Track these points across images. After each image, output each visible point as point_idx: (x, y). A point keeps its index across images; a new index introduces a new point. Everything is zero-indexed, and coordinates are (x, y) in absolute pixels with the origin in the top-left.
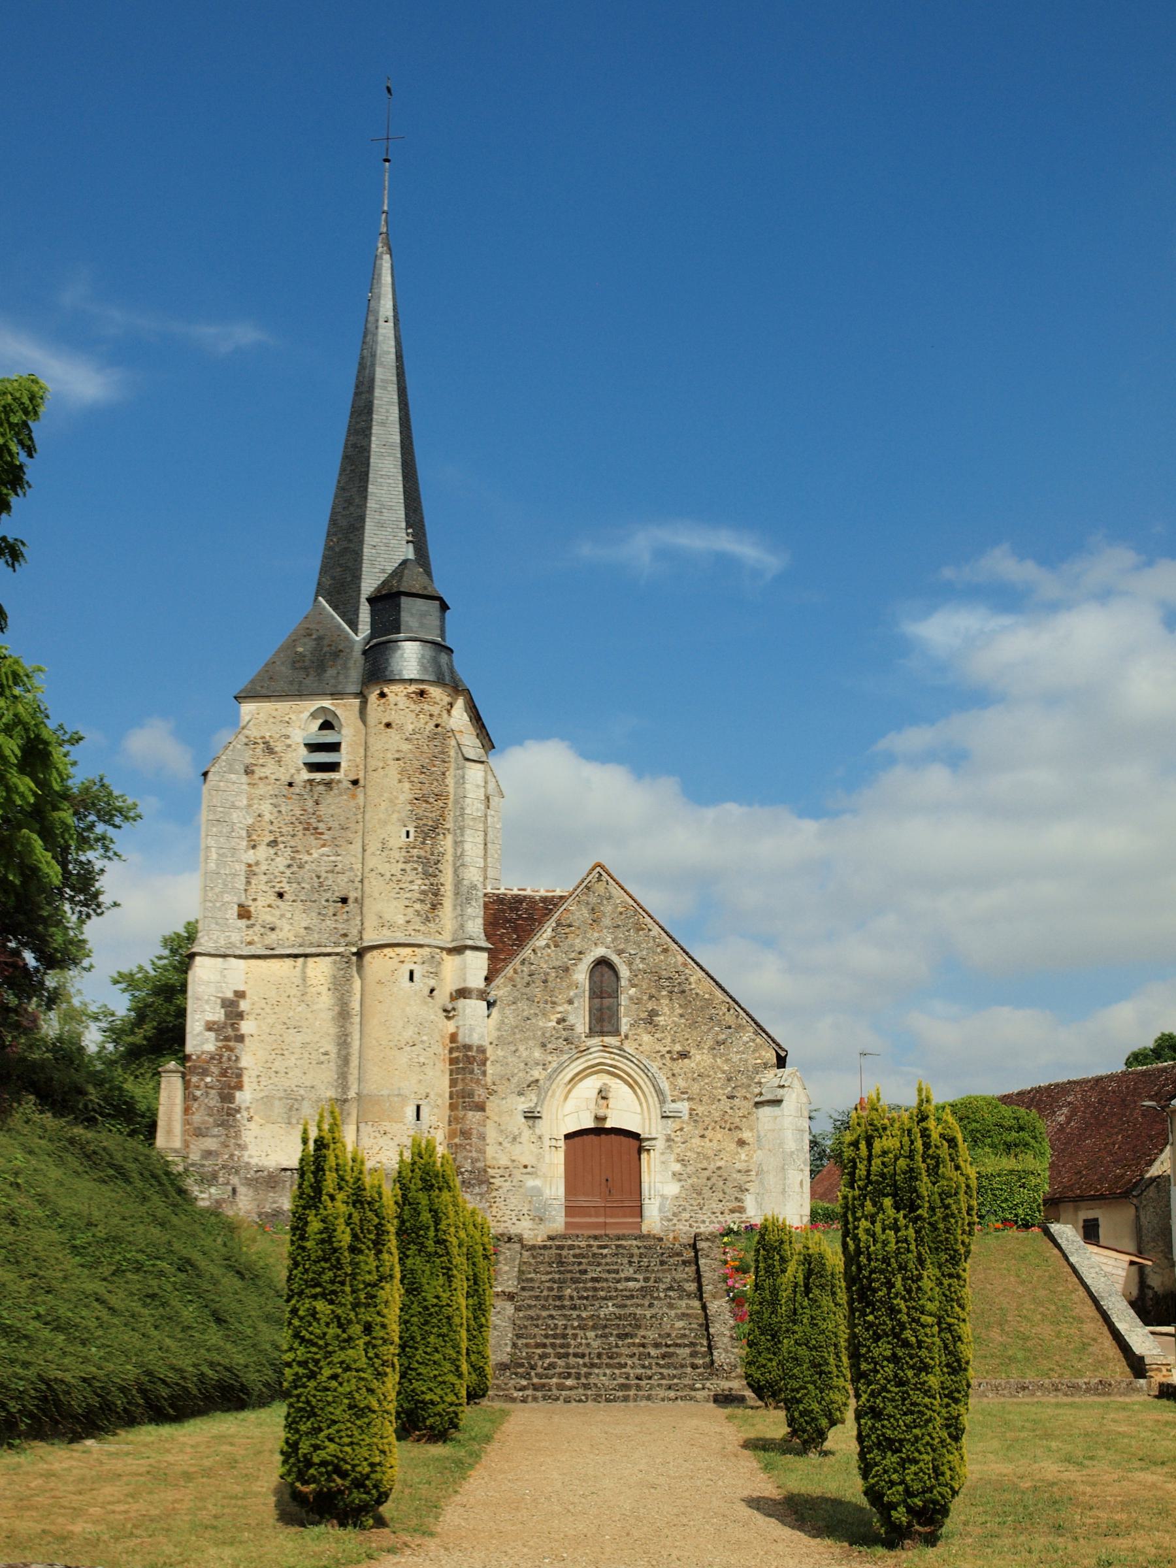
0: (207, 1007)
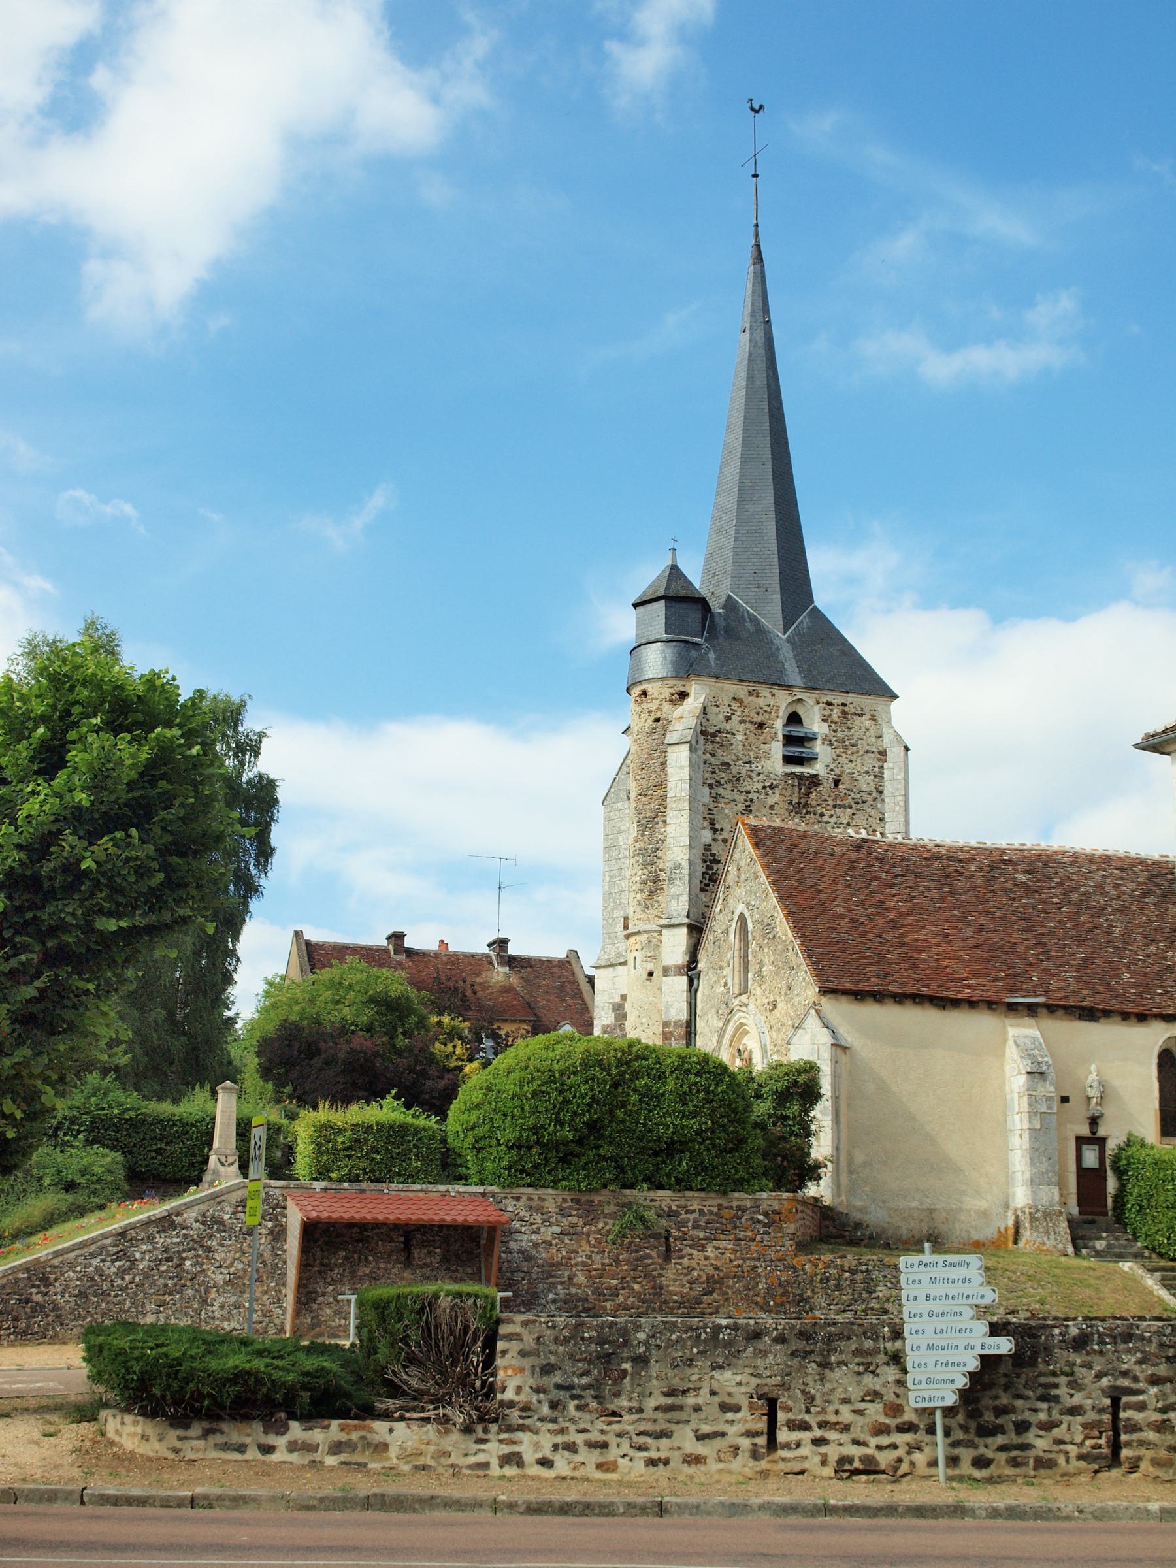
0: (603, 1013)
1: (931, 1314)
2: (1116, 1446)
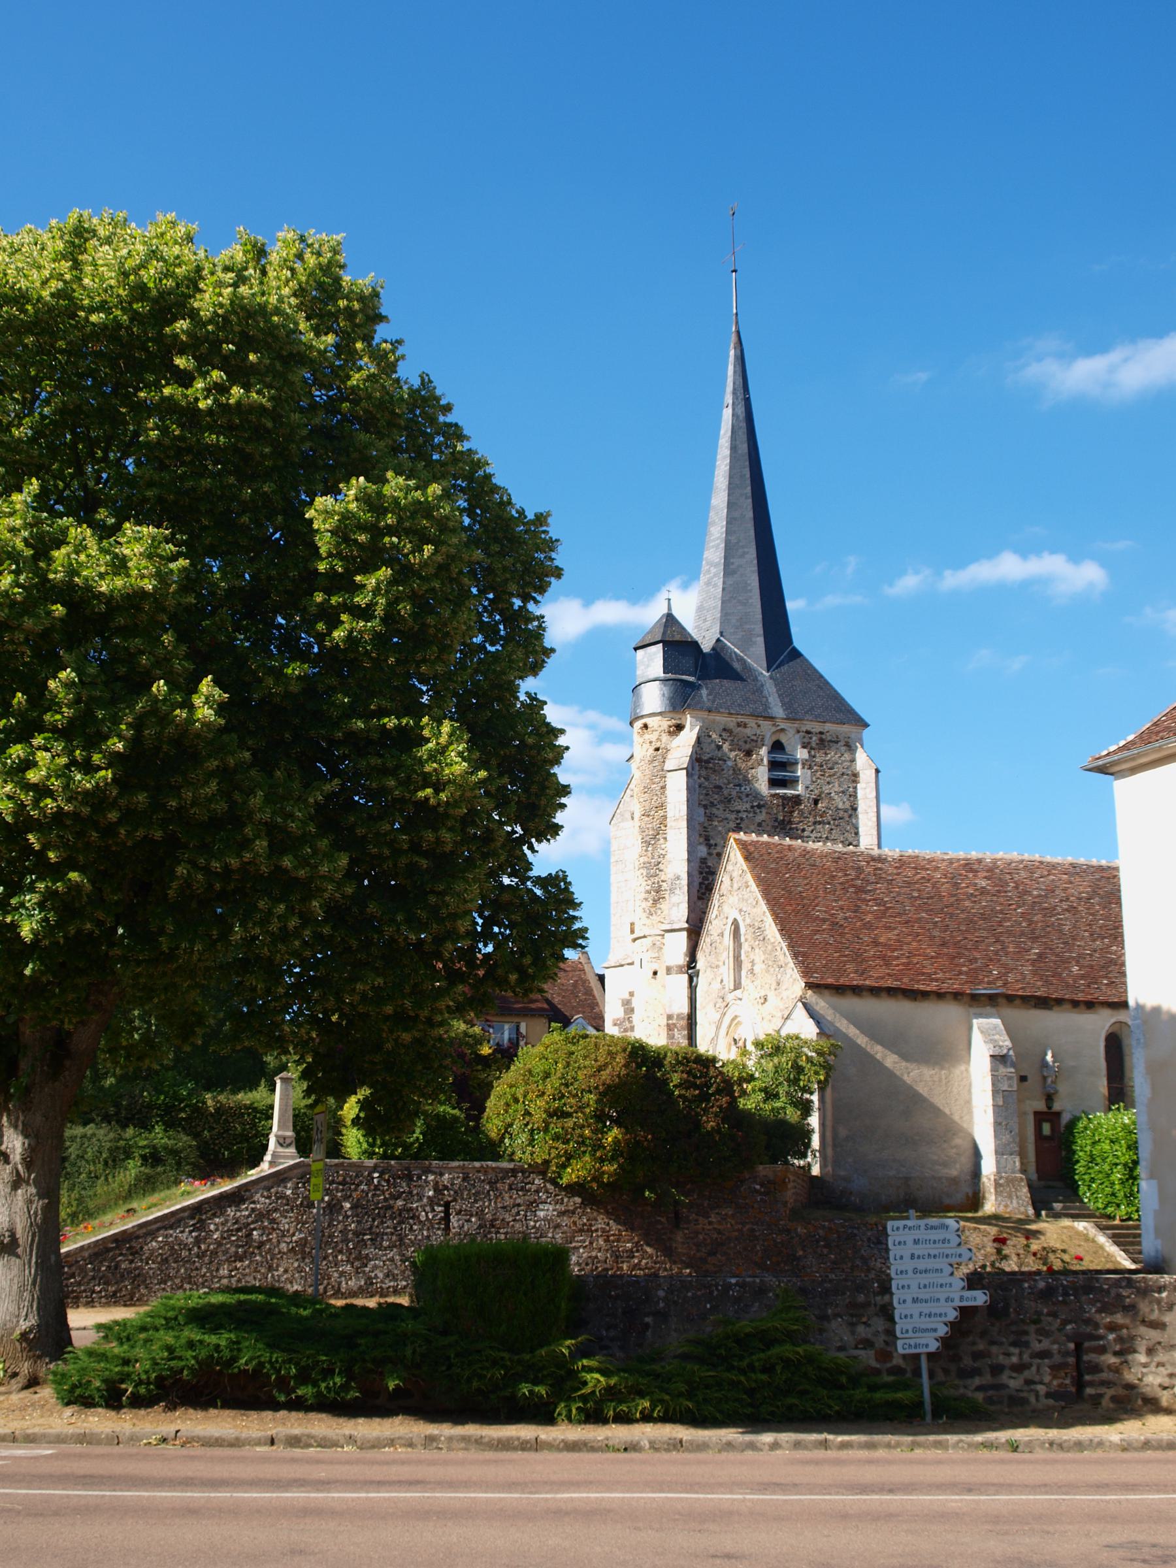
1: (915, 1271)
2: (1080, 1385)
